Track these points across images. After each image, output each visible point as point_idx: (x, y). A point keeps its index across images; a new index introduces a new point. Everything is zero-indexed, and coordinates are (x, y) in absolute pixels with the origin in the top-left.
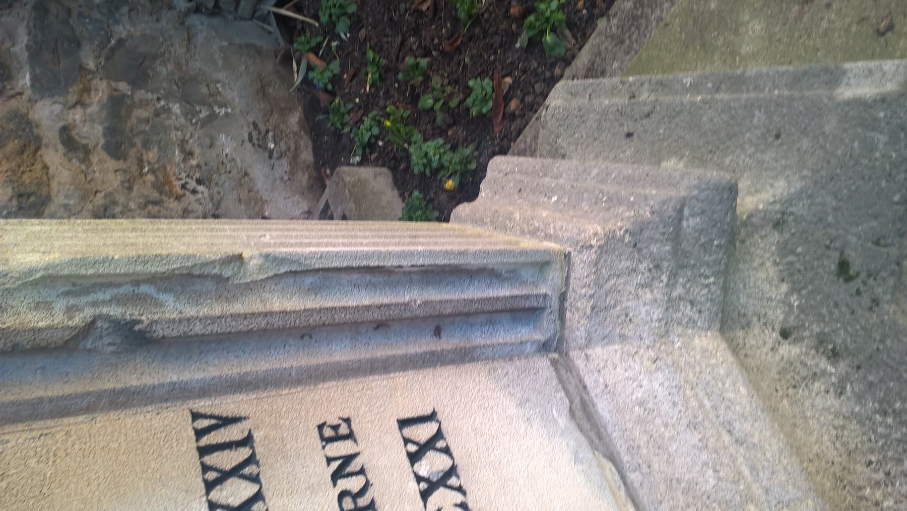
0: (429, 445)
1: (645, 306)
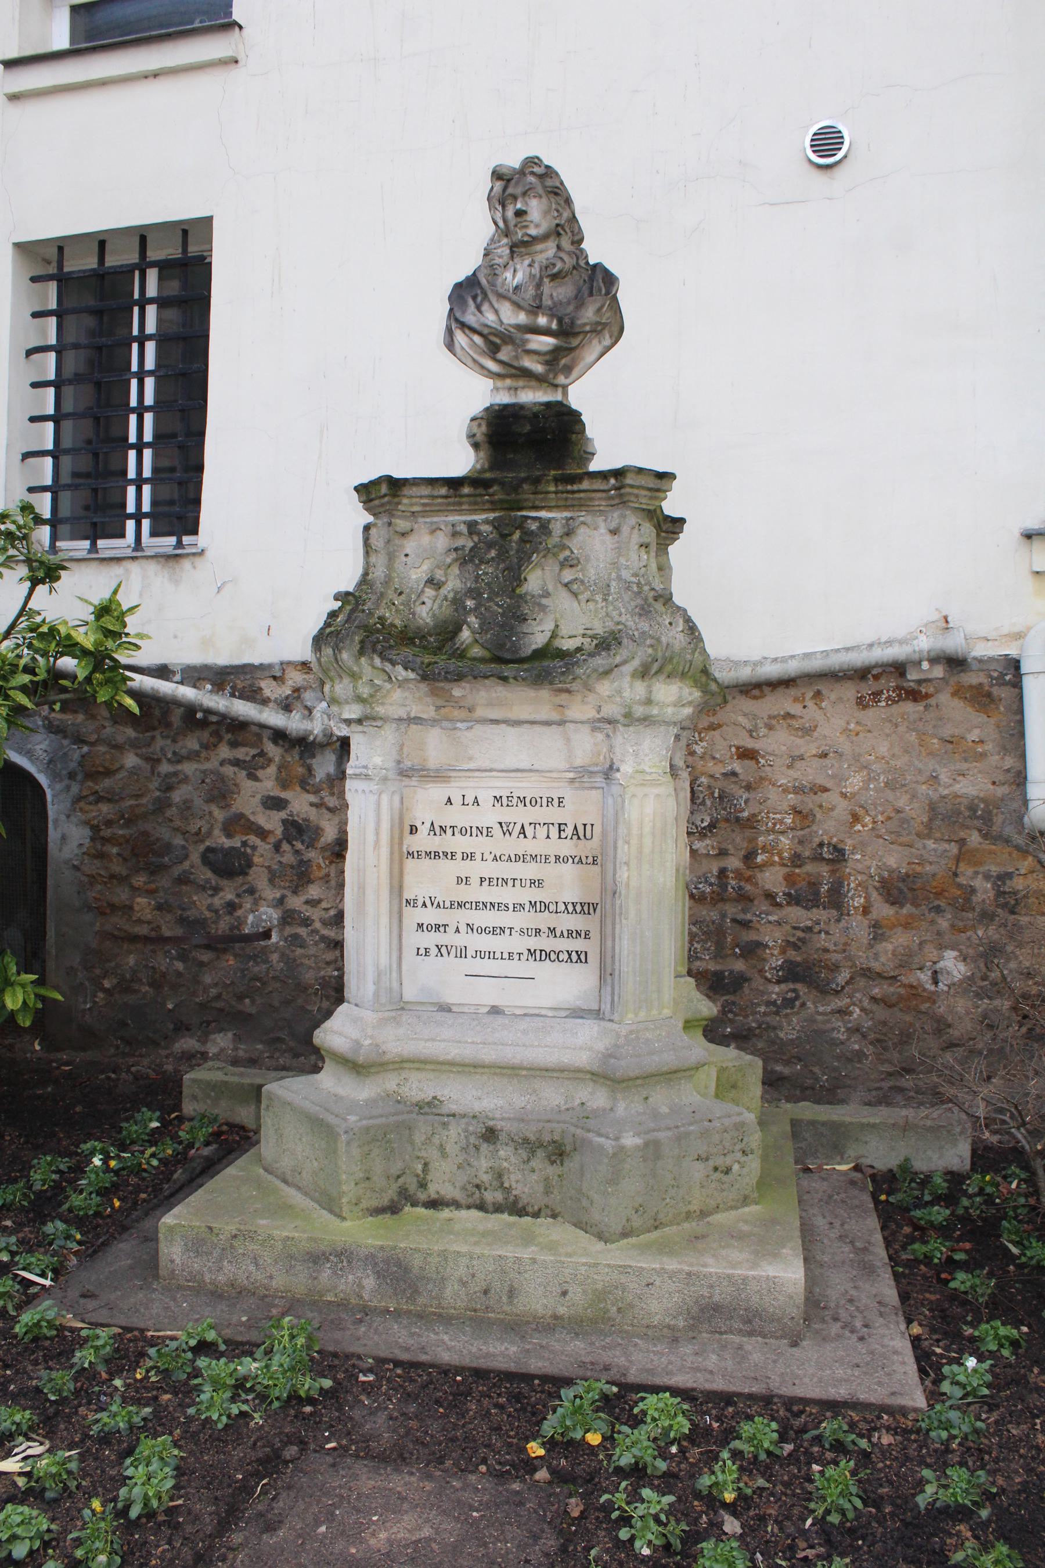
1: (601, 1046)
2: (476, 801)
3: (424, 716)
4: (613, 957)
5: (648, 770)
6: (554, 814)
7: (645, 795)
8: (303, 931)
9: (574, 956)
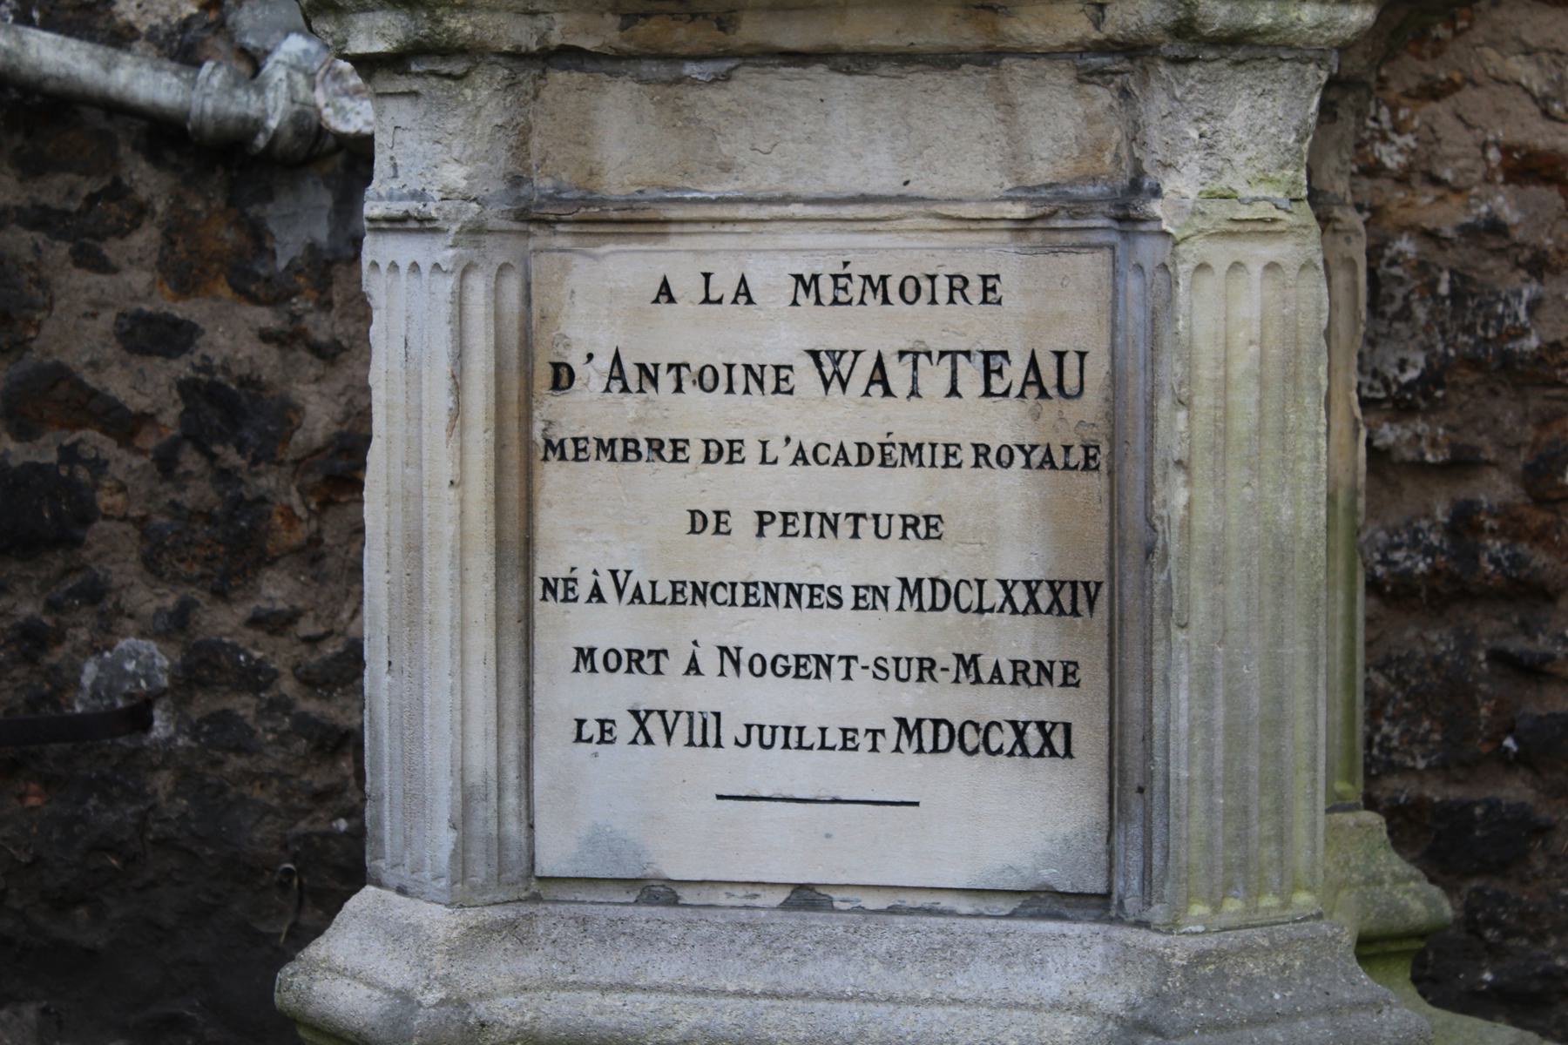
0: (1047, 742)
1: (1112, 998)
2: (743, 291)
3: (589, 44)
4: (1147, 737)
5: (1245, 192)
6: (971, 326)
7: (1237, 266)
8: (243, 705)
9: (1033, 738)
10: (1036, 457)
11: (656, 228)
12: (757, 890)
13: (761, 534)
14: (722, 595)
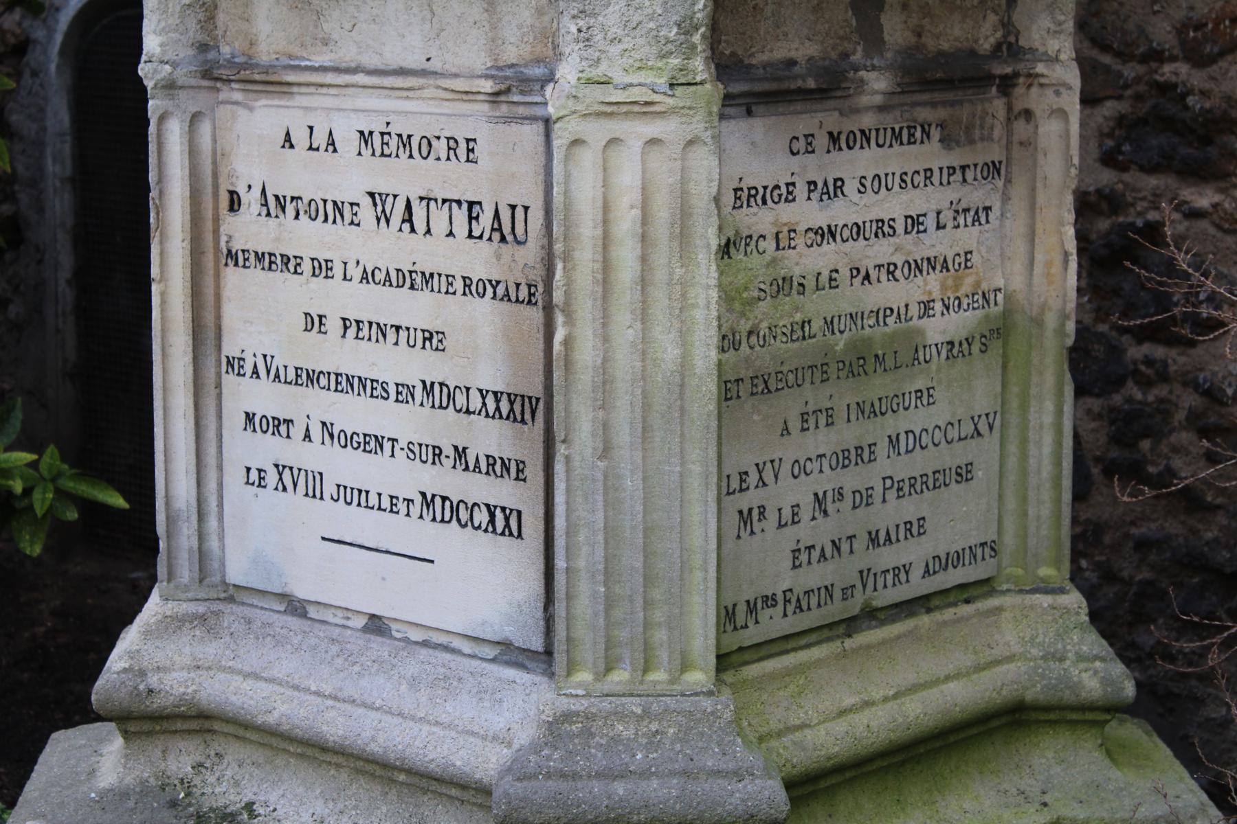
5: (619, 77)
7: (613, 142)
10: (501, 290)
11: (285, 89)
12: (350, 615)
13: (344, 336)
14: (323, 381)
